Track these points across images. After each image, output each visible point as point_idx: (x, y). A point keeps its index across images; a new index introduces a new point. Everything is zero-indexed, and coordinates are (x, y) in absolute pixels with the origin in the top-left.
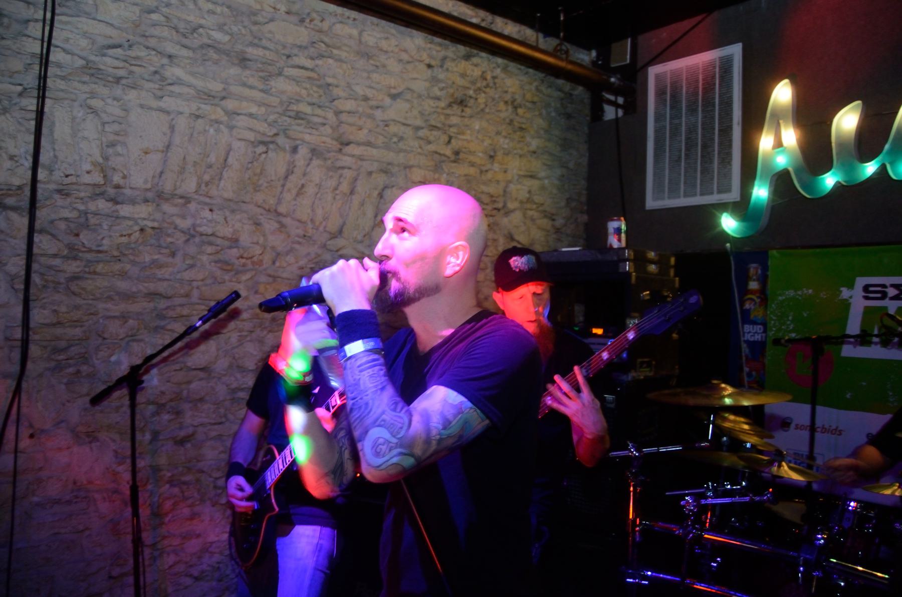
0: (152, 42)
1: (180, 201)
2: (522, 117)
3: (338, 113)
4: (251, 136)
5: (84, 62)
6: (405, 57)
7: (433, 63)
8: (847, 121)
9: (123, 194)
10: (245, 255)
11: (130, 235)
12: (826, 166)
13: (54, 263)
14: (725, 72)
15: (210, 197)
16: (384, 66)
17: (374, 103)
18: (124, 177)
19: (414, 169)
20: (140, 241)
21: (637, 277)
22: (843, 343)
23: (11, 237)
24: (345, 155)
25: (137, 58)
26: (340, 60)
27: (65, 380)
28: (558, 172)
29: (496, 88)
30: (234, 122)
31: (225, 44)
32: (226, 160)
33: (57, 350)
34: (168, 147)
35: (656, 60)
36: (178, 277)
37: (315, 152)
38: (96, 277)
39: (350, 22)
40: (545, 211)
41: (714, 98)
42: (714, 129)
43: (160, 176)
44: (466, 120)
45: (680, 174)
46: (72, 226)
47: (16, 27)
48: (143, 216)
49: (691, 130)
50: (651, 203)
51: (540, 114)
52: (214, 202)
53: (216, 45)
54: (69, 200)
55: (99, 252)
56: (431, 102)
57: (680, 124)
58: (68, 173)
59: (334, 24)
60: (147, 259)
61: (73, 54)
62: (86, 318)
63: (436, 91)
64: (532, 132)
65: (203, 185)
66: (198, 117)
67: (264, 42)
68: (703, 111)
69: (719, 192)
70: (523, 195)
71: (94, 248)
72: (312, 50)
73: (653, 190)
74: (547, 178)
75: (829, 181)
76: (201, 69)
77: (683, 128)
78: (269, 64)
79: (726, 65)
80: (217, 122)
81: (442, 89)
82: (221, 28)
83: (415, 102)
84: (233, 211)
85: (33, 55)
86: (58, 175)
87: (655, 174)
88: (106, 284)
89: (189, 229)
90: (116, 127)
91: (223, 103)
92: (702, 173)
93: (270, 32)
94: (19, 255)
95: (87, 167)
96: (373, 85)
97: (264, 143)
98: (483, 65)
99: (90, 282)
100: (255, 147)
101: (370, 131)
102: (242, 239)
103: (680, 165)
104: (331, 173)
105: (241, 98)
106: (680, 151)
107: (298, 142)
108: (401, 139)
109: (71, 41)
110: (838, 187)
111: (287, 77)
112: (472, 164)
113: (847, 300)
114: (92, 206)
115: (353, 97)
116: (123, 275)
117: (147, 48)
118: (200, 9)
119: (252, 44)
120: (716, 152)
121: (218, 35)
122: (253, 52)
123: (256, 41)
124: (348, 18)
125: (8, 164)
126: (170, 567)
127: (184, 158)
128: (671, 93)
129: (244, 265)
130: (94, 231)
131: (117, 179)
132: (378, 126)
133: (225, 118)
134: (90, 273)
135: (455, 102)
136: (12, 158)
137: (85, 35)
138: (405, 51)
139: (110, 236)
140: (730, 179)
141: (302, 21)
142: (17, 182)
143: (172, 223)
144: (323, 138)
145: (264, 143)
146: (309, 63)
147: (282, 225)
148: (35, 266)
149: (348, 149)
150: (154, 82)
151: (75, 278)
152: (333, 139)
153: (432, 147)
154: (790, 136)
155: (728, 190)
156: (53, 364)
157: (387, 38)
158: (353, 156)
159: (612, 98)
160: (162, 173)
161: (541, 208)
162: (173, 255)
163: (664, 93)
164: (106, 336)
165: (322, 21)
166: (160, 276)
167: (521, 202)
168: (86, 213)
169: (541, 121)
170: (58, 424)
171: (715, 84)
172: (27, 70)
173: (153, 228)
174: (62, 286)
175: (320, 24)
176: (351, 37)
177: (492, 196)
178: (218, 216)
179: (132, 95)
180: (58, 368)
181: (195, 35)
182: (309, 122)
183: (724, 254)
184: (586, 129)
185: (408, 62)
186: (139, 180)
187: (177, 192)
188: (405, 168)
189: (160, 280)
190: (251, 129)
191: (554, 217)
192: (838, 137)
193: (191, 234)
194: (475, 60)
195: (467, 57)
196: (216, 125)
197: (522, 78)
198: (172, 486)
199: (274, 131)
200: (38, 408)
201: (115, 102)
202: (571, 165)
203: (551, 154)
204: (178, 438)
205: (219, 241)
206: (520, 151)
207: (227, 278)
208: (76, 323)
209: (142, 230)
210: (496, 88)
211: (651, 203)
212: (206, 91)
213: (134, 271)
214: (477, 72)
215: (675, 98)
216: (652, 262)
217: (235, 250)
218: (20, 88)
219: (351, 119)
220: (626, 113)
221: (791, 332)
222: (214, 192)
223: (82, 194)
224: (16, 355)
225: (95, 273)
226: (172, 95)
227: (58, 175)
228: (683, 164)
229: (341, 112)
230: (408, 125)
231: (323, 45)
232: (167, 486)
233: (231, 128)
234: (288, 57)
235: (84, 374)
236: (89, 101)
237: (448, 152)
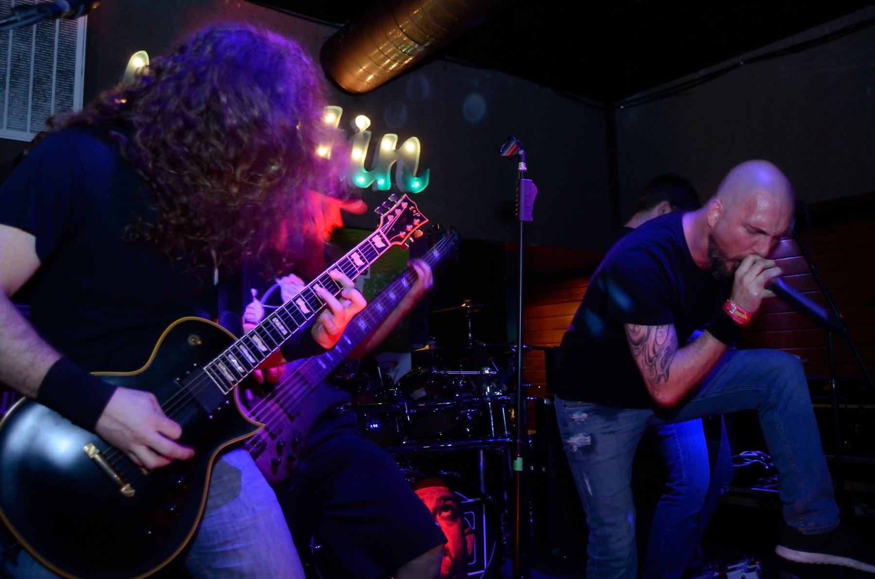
42: (52, 67)
45: (3, 102)
49: (20, 59)
77: (10, 51)
92: (34, 108)
228: (7, 91)
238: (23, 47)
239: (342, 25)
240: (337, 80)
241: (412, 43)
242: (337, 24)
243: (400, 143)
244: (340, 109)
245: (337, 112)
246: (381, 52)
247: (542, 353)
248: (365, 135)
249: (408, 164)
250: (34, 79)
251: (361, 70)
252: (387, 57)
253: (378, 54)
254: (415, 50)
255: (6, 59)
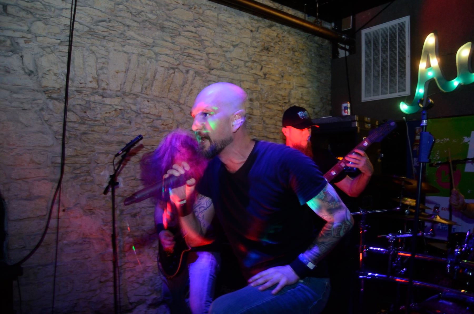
0: (120, 19)
1: (134, 96)
2: (297, 57)
3: (208, 54)
4: (167, 65)
5: (88, 29)
6: (240, 26)
7: (253, 29)
8: (464, 52)
9: (106, 93)
10: (165, 124)
11: (110, 113)
12: (454, 76)
13: (75, 126)
15: (147, 95)
16: (230, 31)
17: (225, 49)
18: (107, 84)
19: (245, 82)
20: (115, 116)
21: (360, 130)
22: (465, 163)
23: (55, 113)
24: (211, 75)
25: (113, 27)
26: (209, 28)
27: (80, 183)
28: (316, 84)
29: (284, 42)
30: (159, 58)
31: (154, 20)
32: (154, 77)
33: (76, 169)
34: (127, 70)
35: (364, 27)
36: (133, 134)
37: (197, 73)
38: (94, 133)
39: (213, 9)
40: (310, 104)
41: (396, 44)
42: (396, 60)
43: (124, 84)
44: (270, 58)
46: (83, 108)
47: (57, 12)
48: (116, 103)
49: (384, 61)
50: (364, 98)
51: (307, 56)
52: (149, 97)
53: (150, 20)
54: (81, 95)
55: (96, 121)
56: (252, 49)
57: (379, 58)
58: (81, 82)
59: (205, 10)
60: (118, 124)
61: (83, 25)
62: (89, 153)
63: (255, 44)
64: (303, 64)
65: (144, 89)
66: (142, 55)
67: (173, 19)
68: (390, 51)
69: (399, 91)
70: (299, 96)
71: (94, 119)
72: (195, 23)
73: (365, 91)
74: (310, 87)
75: (455, 83)
76: (143, 32)
78: (175, 30)
79: (402, 27)
80: (151, 58)
81: (258, 43)
82: (151, 12)
83: (245, 48)
84: (158, 102)
85: (65, 25)
86: (76, 83)
87: (366, 84)
88: (99, 137)
89: (137, 110)
90: (103, 60)
91: (153, 49)
92: (390, 82)
93: (175, 14)
94: (58, 122)
95: (90, 79)
96: (224, 40)
97: (173, 68)
98: (278, 30)
99: (92, 135)
100: (168, 70)
101: (223, 63)
102: (162, 116)
103: (379, 79)
104: (204, 84)
105: (162, 46)
106: (379, 71)
107: (189, 68)
108: (238, 67)
109: (83, 19)
110: (460, 86)
111: (183, 36)
112: (273, 80)
113: (467, 143)
114: (92, 99)
115: (215, 46)
116: (107, 132)
117: (118, 22)
118: (142, 3)
119: (167, 20)
120: (397, 71)
121: (150, 16)
122: (167, 24)
123: (168, 18)
124: (212, 7)
125: (54, 77)
126: (129, 277)
127: (135, 76)
128: (373, 42)
129: (164, 129)
130: (94, 110)
131: (103, 85)
132: (227, 60)
133: (154, 56)
134: (92, 131)
135: (264, 49)
136: (55, 74)
137: (89, 15)
138: (239, 23)
139: (101, 113)
140: (405, 85)
141: (190, 8)
142: (58, 86)
143: (130, 107)
144: (201, 66)
145: (173, 68)
146: (194, 30)
147: (182, 109)
148: (67, 128)
149: (213, 72)
150: (121, 39)
151: (84, 133)
152: (205, 67)
153: (253, 71)
154: (435, 62)
155: (404, 90)
156: (74, 175)
157: (230, 17)
158: (215, 75)
159: (343, 46)
160: (125, 82)
161: (308, 103)
162: (130, 122)
163: (370, 43)
164: (99, 162)
165: (200, 8)
166: (123, 133)
167: (298, 99)
168: (89, 102)
169: (307, 59)
170: (76, 205)
171: (396, 37)
172: (62, 32)
173: (120, 110)
174: (79, 137)
175: (199, 10)
176: (214, 16)
177: (283, 96)
178: (151, 104)
179: (111, 45)
180: (76, 177)
181: (140, 15)
182: (194, 58)
183: (403, 122)
184: (330, 63)
185: (242, 29)
186: (114, 85)
187: (132, 92)
188: (240, 81)
189: (124, 135)
190: (166, 62)
191: (315, 107)
192: (459, 61)
193: (138, 113)
194: (274, 28)
195: (270, 26)
196: (150, 59)
197: (297, 37)
198: (130, 237)
199: (178, 62)
200: (68, 197)
201: (103, 48)
202: (322, 81)
203: (312, 75)
204: (133, 214)
205: (152, 117)
206: (297, 75)
207: (156, 134)
208: (85, 155)
209: (116, 110)
210: (284, 42)
211: (364, 98)
212: (145, 43)
213: (111, 130)
214: (275, 34)
215: (376, 45)
216: (368, 123)
217: (160, 121)
218: (59, 41)
219: (214, 58)
220: (350, 53)
221: (438, 160)
222: (149, 93)
223: (88, 93)
224: (58, 171)
225: (94, 131)
226: (129, 44)
227: (76, 83)
229: (209, 54)
230: (242, 60)
231: (200, 20)
232: (127, 237)
233: (157, 61)
234: (184, 26)
235: (89, 180)
236: (91, 48)
237: (261, 74)
238: (385, 55)
250: (390, 69)
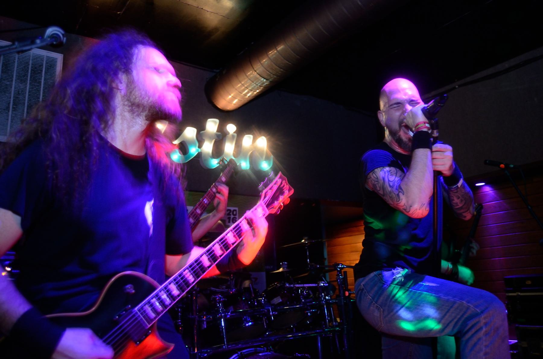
14: (50, 66)
41: (41, 79)
45: (8, 120)
49: (19, 93)
68: (30, 83)
106: (9, 104)
171: (42, 71)
238: (22, 86)
239: (218, 71)
240: (215, 103)
241: (263, 79)
242: (215, 70)
243: (254, 140)
244: (217, 121)
245: (215, 122)
246: (243, 85)
247: (352, 270)
248: (233, 136)
249: (261, 153)
250: (28, 106)
251: (230, 97)
252: (247, 88)
253: (241, 87)
254: (264, 83)
255: (10, 93)
